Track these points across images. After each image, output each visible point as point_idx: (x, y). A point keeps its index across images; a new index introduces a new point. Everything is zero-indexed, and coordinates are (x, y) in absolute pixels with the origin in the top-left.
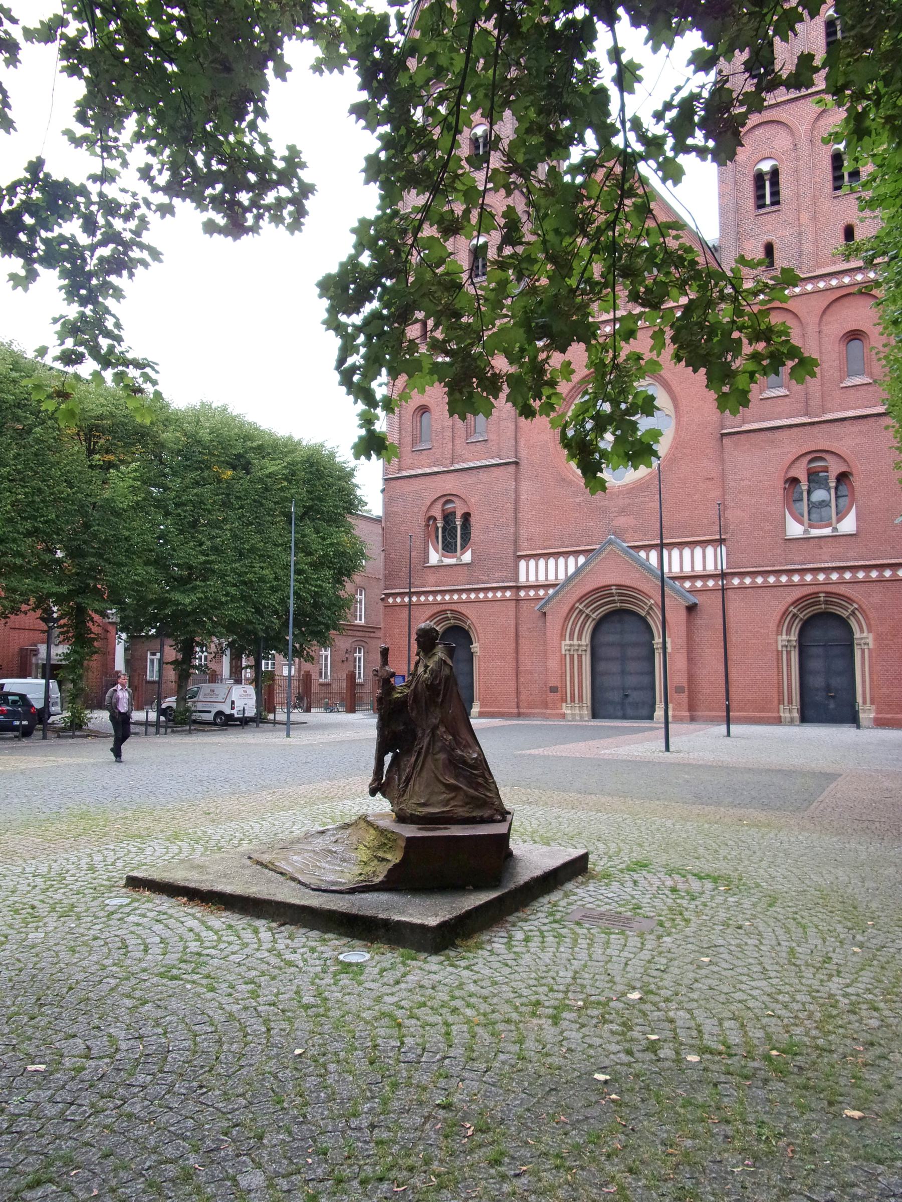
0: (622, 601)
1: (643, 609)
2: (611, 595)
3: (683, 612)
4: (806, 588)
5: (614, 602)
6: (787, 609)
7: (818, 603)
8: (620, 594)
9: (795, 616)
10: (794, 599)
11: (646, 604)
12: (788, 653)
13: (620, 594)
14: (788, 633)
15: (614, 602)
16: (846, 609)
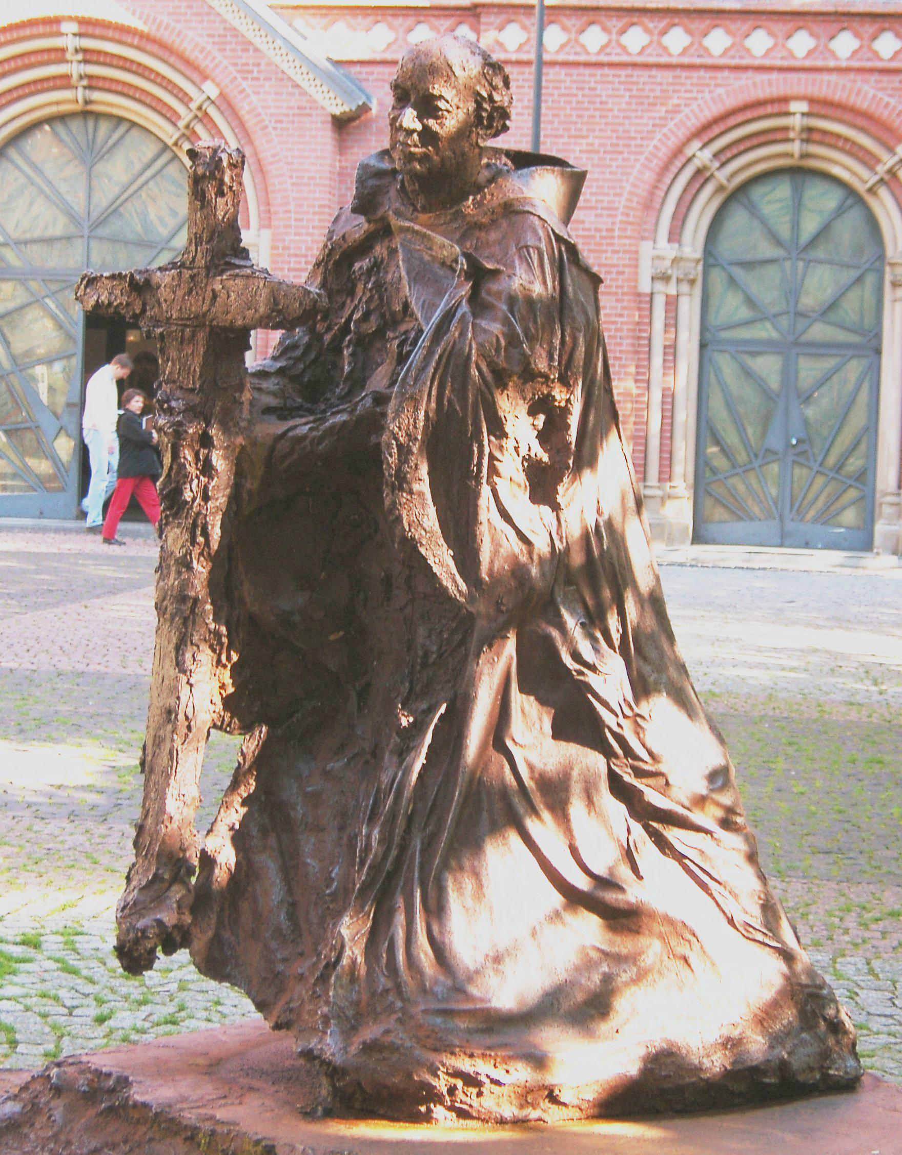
0: (93, 83)
1: (171, 117)
2: (58, 56)
3: (326, 136)
4: (746, 79)
5: (63, 82)
6: (679, 151)
7: (779, 135)
8: (89, 57)
9: (701, 176)
10: (708, 114)
11: (185, 98)
12: (672, 304)
13: (89, 57)
14: (675, 235)
15: (63, 82)
16: (868, 160)
